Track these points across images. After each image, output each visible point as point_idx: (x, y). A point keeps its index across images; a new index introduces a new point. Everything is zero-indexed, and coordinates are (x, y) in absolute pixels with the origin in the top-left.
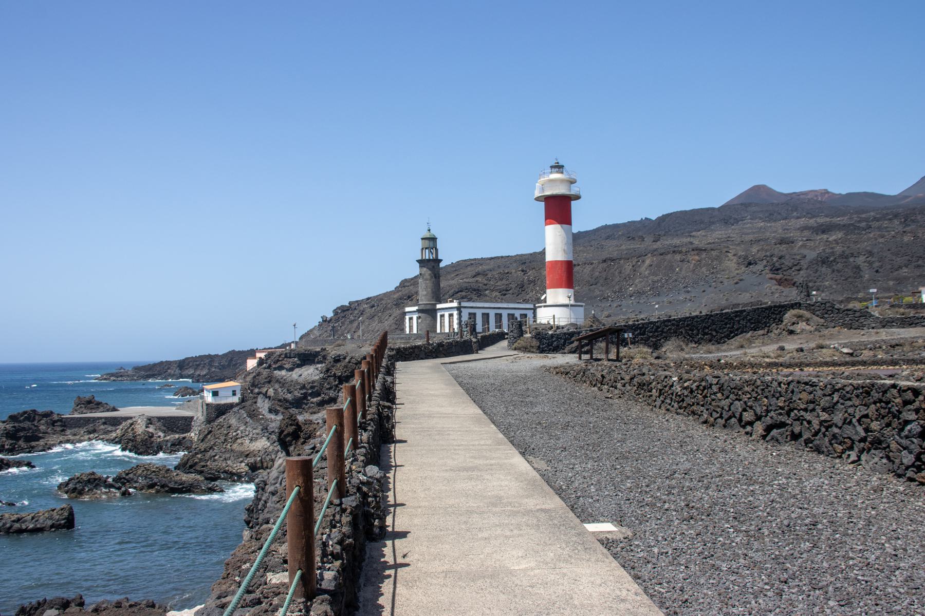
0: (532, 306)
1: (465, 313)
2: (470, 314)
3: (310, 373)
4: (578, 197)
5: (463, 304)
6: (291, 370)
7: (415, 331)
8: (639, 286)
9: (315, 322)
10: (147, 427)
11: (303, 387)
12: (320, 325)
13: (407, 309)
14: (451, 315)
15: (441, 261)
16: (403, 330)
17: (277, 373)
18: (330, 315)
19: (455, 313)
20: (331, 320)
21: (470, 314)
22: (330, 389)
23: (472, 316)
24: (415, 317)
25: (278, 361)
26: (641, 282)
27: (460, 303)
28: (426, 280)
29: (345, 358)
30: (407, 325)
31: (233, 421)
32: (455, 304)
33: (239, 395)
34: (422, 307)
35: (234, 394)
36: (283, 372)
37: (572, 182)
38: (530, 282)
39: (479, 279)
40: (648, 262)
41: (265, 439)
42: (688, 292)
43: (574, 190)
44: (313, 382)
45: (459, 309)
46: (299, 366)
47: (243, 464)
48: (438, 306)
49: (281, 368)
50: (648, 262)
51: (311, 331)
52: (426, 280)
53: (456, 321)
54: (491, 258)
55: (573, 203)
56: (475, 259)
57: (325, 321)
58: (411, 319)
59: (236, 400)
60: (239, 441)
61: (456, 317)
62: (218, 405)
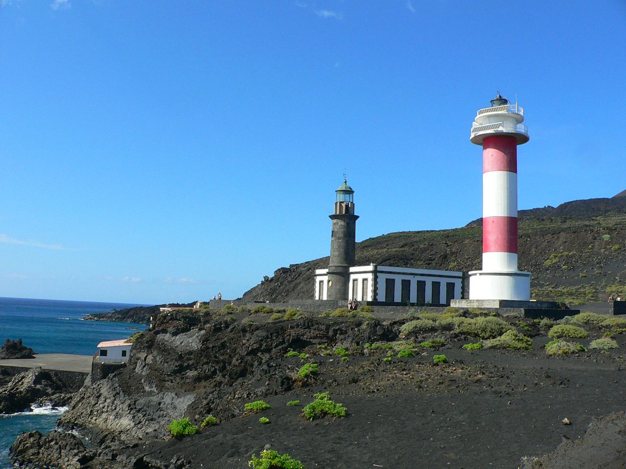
0: (460, 274)
1: (382, 278)
2: (387, 280)
3: (191, 341)
4: (524, 139)
5: (380, 268)
6: (175, 334)
7: (325, 298)
8: (554, 261)
9: (258, 281)
10: (35, 382)
11: (181, 357)
12: (263, 283)
13: (318, 272)
14: (365, 280)
15: (357, 217)
16: (313, 296)
17: (160, 337)
18: (271, 275)
19: (370, 277)
20: (272, 279)
21: (387, 280)
22: (207, 363)
23: (390, 284)
24: (325, 279)
25: (162, 323)
26: (555, 257)
27: (376, 267)
28: (339, 238)
29: (227, 326)
30: (317, 289)
31: (104, 391)
32: (370, 268)
33: (127, 358)
34: (333, 269)
35: (124, 354)
36: (167, 336)
37: (519, 120)
38: (453, 253)
39: (406, 248)
40: (562, 239)
41: (130, 416)
42: (601, 267)
43: (521, 129)
44: (190, 353)
45: (375, 272)
46: (185, 330)
47: (77, 458)
48: (352, 269)
49: (165, 331)
50: (562, 239)
51: (254, 289)
52: (339, 238)
53: (370, 288)
54: (419, 232)
55: (519, 147)
56: (404, 232)
57: (267, 280)
58: (321, 282)
59: (125, 360)
60: (104, 415)
61: (370, 283)
62: (104, 365)
